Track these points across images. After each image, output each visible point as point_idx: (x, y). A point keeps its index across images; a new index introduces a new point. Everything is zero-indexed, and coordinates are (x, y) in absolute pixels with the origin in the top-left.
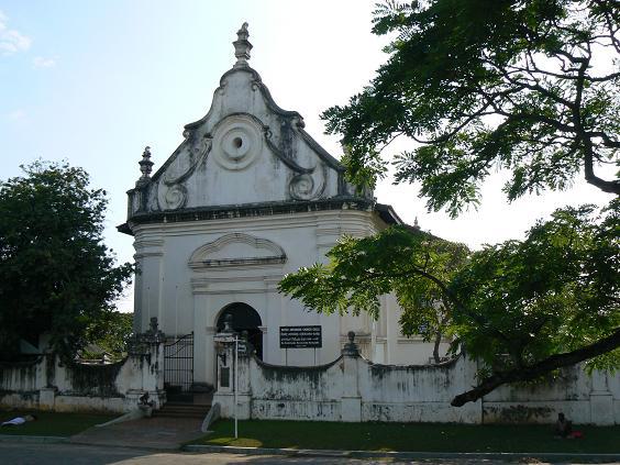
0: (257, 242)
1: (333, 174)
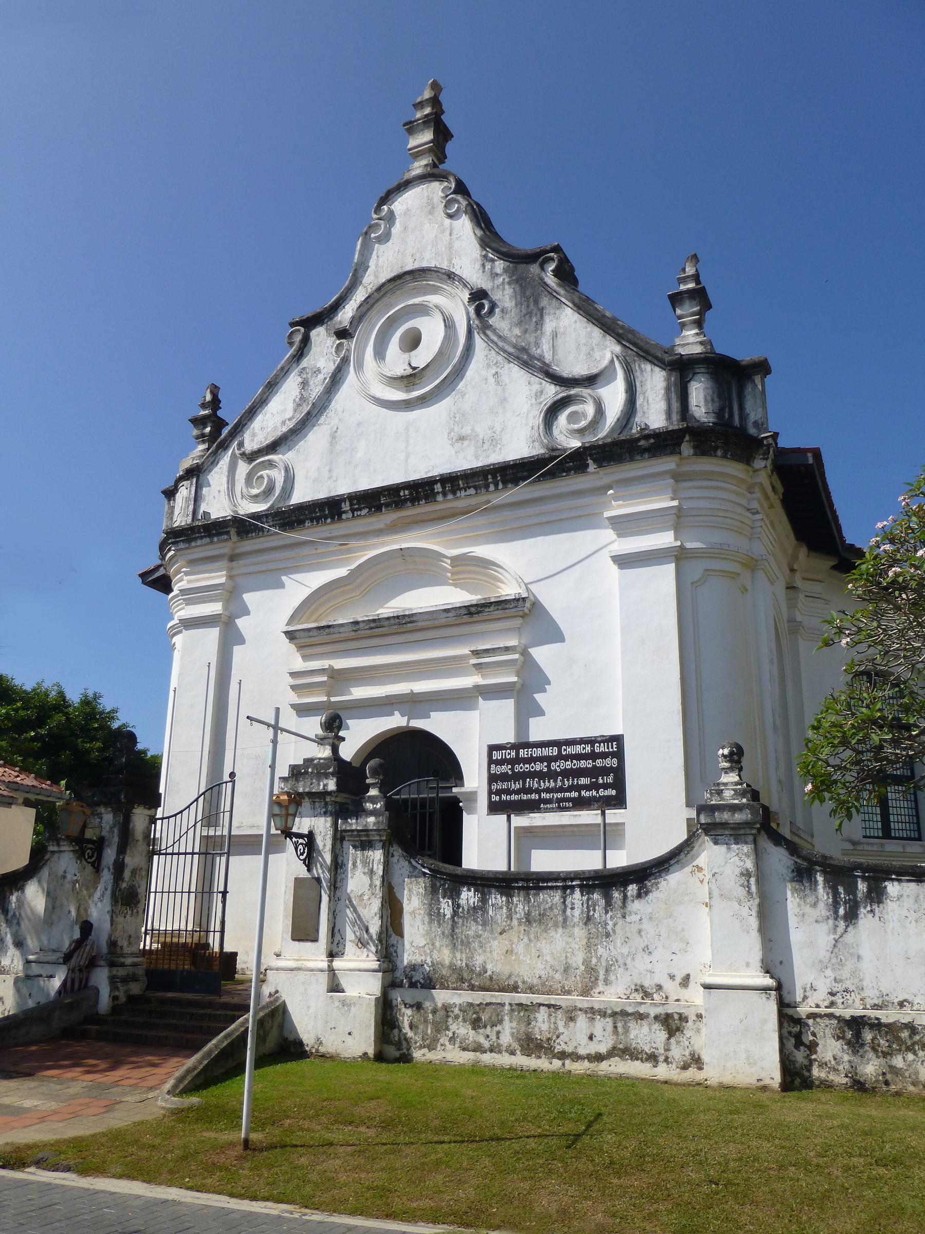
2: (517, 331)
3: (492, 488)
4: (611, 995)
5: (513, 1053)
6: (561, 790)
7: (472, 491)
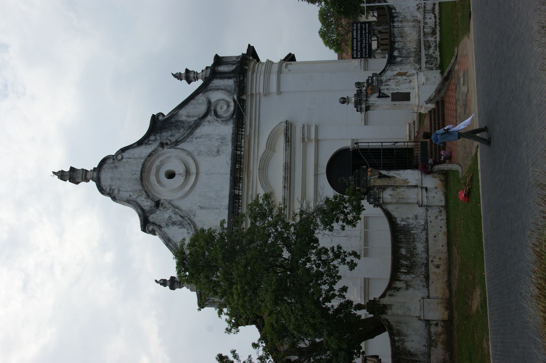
0: (271, 146)
1: (217, 82)
2: (182, 130)
3: (243, 133)
4: (420, 16)
5: (436, 37)
6: (366, 38)
7: (243, 140)
